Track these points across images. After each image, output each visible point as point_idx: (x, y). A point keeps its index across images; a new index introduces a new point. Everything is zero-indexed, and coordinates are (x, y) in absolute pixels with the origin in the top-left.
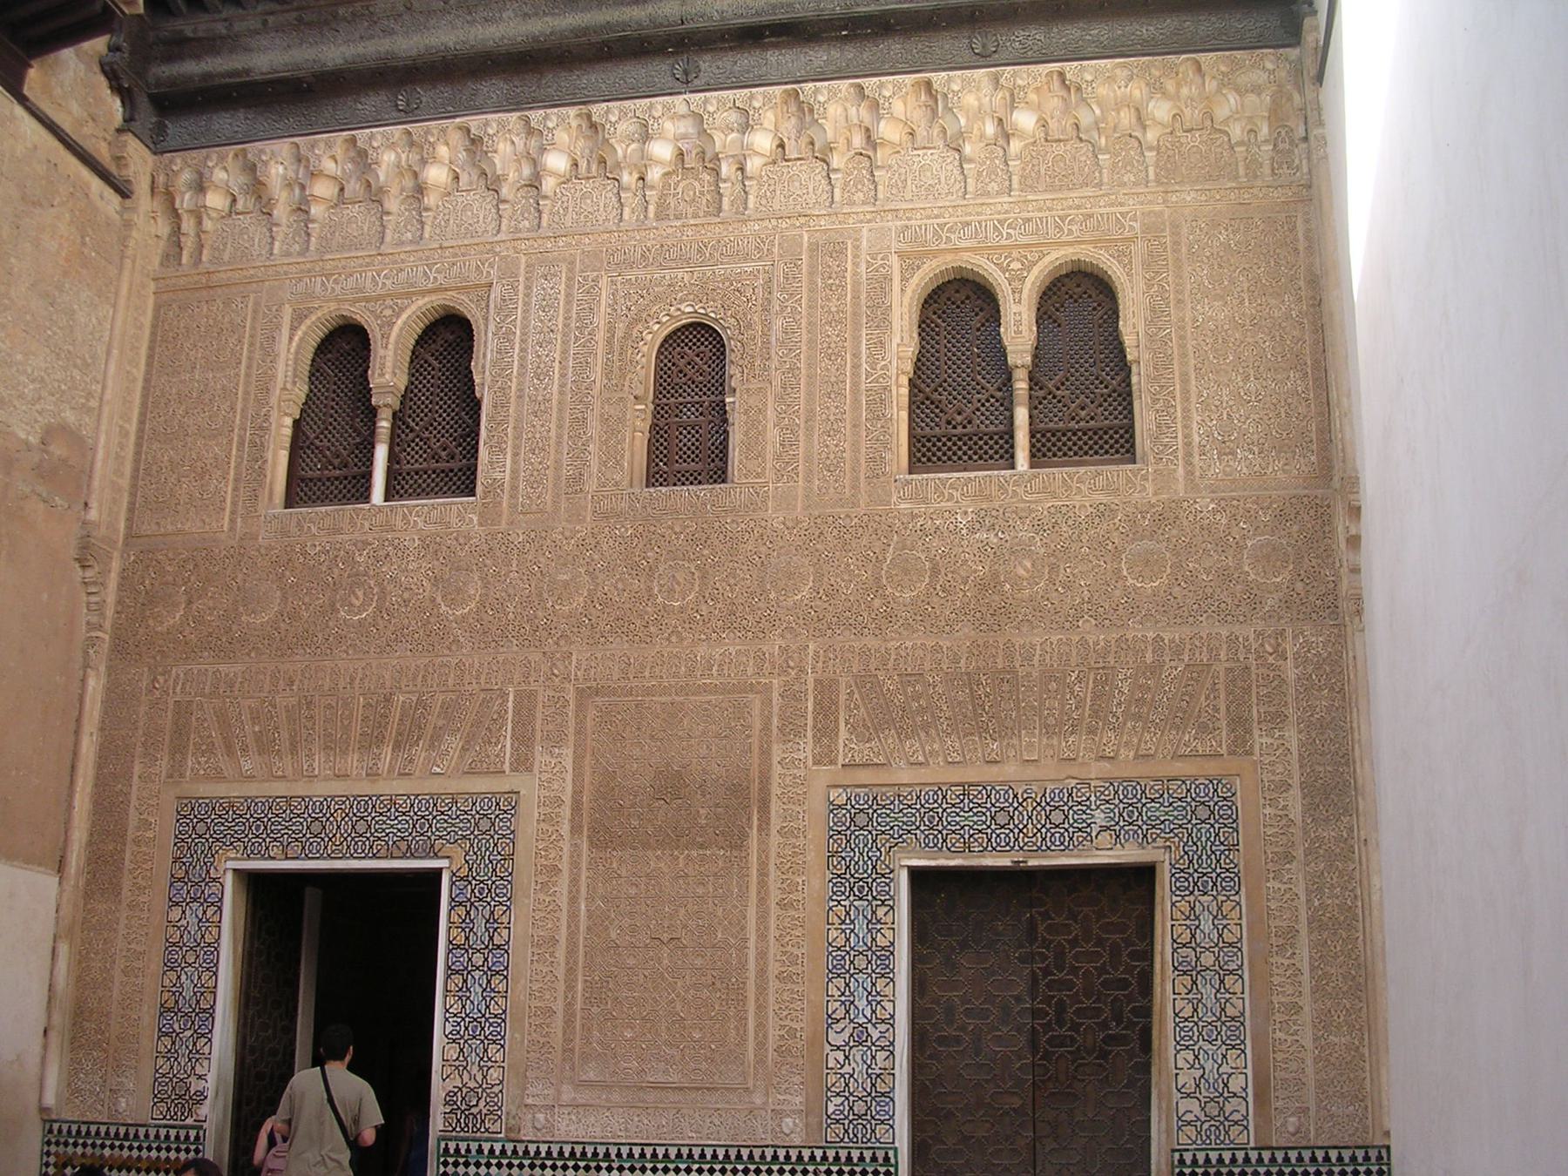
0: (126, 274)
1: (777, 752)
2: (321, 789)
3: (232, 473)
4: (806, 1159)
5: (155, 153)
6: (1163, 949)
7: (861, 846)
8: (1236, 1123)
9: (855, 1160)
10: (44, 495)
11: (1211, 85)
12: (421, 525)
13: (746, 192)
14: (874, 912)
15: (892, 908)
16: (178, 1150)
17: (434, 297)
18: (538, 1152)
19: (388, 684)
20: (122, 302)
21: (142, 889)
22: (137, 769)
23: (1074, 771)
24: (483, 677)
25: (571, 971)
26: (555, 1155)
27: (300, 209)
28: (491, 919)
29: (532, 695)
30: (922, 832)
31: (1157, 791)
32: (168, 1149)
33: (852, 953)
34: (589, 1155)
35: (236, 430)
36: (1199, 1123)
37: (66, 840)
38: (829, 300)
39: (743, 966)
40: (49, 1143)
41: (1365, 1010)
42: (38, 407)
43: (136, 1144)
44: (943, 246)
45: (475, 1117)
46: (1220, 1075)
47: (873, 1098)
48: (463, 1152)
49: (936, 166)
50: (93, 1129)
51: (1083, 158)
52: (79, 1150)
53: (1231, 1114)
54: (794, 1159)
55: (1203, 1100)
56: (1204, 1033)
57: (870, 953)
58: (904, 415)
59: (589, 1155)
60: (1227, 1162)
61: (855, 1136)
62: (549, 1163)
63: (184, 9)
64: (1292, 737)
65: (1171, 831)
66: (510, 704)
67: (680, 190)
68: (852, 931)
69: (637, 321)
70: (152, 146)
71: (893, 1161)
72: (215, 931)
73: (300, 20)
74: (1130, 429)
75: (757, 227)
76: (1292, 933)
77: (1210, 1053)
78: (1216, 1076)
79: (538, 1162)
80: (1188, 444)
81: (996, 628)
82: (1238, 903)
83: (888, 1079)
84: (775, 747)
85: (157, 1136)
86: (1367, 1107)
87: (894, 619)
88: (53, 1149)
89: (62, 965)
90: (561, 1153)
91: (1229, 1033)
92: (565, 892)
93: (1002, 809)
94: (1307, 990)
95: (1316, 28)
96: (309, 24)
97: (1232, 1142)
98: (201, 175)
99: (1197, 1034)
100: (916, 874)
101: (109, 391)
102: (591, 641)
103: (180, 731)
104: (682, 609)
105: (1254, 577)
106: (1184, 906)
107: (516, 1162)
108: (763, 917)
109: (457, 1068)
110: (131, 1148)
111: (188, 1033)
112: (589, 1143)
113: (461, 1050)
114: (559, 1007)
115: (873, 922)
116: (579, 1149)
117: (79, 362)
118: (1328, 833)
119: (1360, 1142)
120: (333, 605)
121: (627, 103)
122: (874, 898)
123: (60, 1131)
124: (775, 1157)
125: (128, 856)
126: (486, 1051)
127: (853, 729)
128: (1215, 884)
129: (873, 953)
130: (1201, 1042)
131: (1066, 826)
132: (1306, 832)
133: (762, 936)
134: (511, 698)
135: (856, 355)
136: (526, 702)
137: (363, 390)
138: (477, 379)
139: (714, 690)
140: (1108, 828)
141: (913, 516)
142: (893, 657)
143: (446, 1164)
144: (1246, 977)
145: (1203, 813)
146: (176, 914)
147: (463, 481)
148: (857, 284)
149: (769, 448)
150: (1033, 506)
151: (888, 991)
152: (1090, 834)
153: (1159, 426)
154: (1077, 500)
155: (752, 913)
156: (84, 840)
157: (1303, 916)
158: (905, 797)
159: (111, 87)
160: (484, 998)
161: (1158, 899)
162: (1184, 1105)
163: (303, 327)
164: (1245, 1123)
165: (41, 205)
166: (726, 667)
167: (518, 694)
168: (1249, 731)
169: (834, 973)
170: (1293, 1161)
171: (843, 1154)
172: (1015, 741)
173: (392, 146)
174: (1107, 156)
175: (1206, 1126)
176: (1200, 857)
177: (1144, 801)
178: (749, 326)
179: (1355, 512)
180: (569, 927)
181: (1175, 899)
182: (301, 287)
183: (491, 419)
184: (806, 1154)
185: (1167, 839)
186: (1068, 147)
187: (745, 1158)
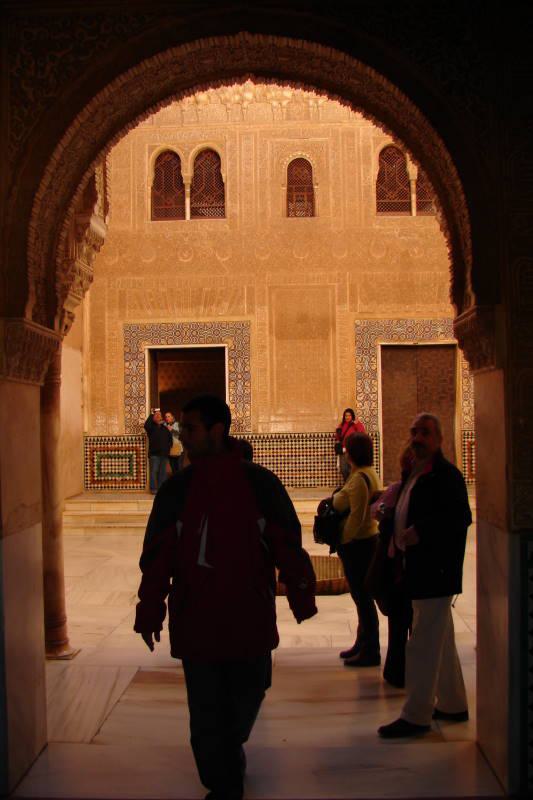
1: (337, 308)
2: (178, 321)
22: (107, 314)
25: (272, 379)
28: (244, 364)
39: (329, 377)
100: (383, 347)
108: (335, 361)
125: (107, 345)
127: (362, 301)
133: (335, 366)
135: (360, 174)
136: (251, 291)
138: (223, 175)
146: (127, 364)
155: (331, 360)
167: (248, 288)
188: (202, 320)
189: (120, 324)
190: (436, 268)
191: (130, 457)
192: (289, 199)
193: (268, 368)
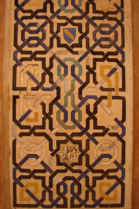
8: (105, 174)
36: (47, 175)
46: (83, 100)
53: (98, 160)
55: (55, 139)
56: (61, 35)
77: (69, 64)
78: (78, 102)
91: (99, 36)
99: (49, 35)
130: (55, 49)
164: (119, 174)
175: (58, 179)
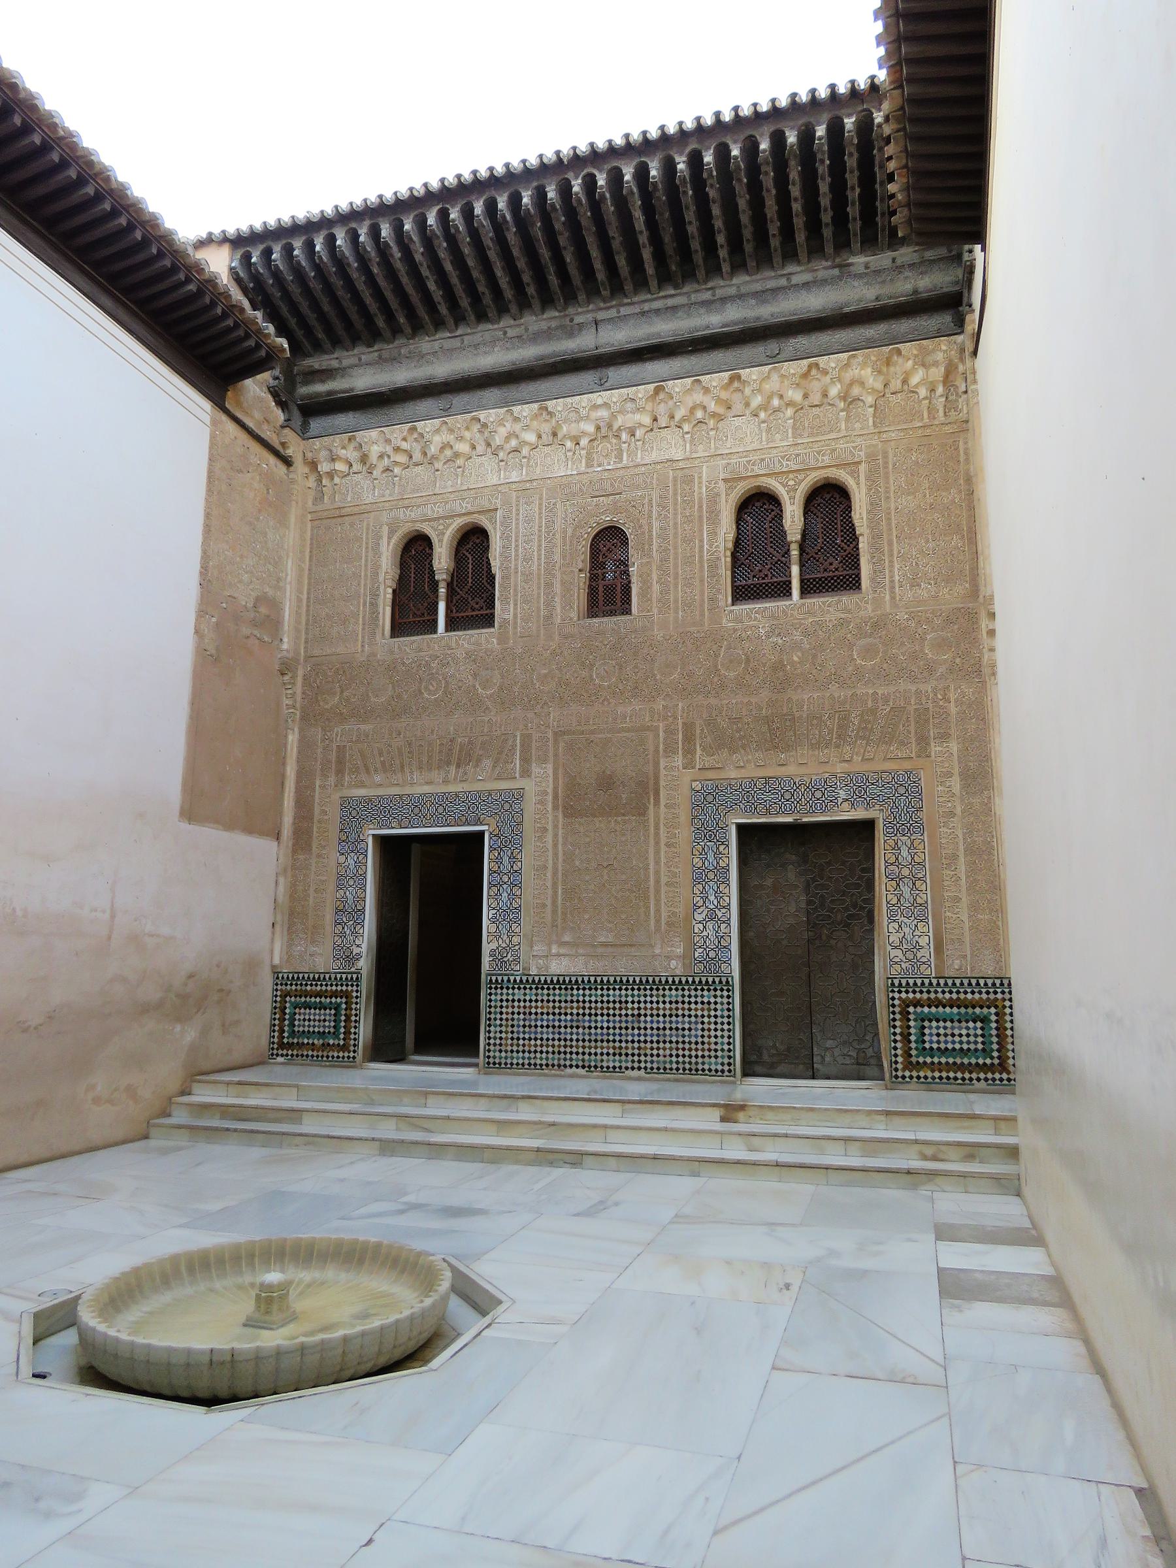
0: (293, 510)
1: (662, 763)
3: (361, 621)
4: (684, 982)
5: (304, 439)
6: (879, 864)
7: (710, 812)
8: (924, 963)
9: (710, 983)
10: (258, 635)
11: (910, 363)
12: (466, 646)
13: (637, 449)
14: (718, 848)
15: (728, 846)
16: (347, 985)
17: (465, 518)
18: (540, 981)
19: (452, 733)
20: (292, 526)
21: (324, 847)
22: (318, 783)
23: (828, 768)
24: (503, 727)
25: (555, 885)
26: (549, 982)
27: (388, 469)
28: (512, 858)
29: (529, 736)
30: (743, 804)
31: (875, 779)
32: (342, 985)
33: (706, 871)
34: (567, 982)
35: (362, 597)
37: (281, 823)
38: (685, 509)
39: (647, 879)
40: (277, 984)
41: (999, 900)
42: (251, 587)
43: (324, 983)
44: (751, 474)
45: (506, 962)
46: (914, 936)
47: (719, 949)
48: (500, 981)
49: (744, 426)
50: (301, 976)
51: (830, 415)
52: (294, 987)
54: (677, 982)
55: (904, 950)
57: (716, 871)
58: (729, 573)
59: (567, 982)
60: (919, 985)
61: (710, 969)
62: (546, 986)
63: (312, 352)
64: (954, 747)
65: (883, 801)
66: (518, 741)
67: (599, 449)
68: (706, 858)
69: (577, 527)
70: (301, 434)
71: (731, 983)
72: (364, 868)
73: (380, 357)
74: (858, 576)
75: (643, 469)
76: (955, 857)
79: (540, 986)
80: (892, 581)
81: (782, 690)
82: (923, 840)
83: (727, 939)
84: (662, 761)
85: (336, 978)
86: (1001, 955)
87: (725, 688)
88: (279, 987)
89: (281, 888)
90: (552, 981)
92: (551, 841)
93: (787, 790)
94: (964, 889)
95: (974, 321)
96: (386, 361)
97: (921, 974)
98: (331, 451)
100: (741, 828)
101: (289, 577)
102: (560, 706)
103: (340, 762)
104: (609, 687)
105: (930, 656)
106: (891, 842)
107: (528, 986)
108: (657, 852)
109: (496, 937)
110: (321, 985)
111: (351, 923)
112: (567, 975)
113: (498, 927)
114: (549, 902)
115: (718, 855)
116: (561, 979)
117: (272, 561)
118: (976, 801)
119: (997, 975)
120: (420, 691)
121: (569, 400)
122: (718, 841)
123: (283, 978)
124: (667, 982)
125: (315, 829)
126: (511, 927)
127: (704, 749)
128: (909, 830)
129: (718, 870)
131: (823, 799)
132: (962, 800)
133: (657, 863)
134: (518, 738)
135: (701, 541)
136: (526, 740)
137: (432, 573)
139: (628, 730)
140: (847, 800)
141: (735, 630)
142: (725, 709)
143: (491, 988)
144: (928, 881)
145: (902, 790)
147: (488, 620)
148: (700, 499)
149: (654, 595)
150: (803, 621)
151: (727, 891)
152: (837, 804)
153: (875, 572)
154: (828, 617)
155: (651, 850)
156: (291, 821)
157: (961, 848)
158: (733, 786)
159: (275, 402)
160: (509, 899)
161: (876, 839)
162: (894, 953)
163: (395, 537)
165: (242, 472)
166: (634, 717)
167: (522, 735)
168: (928, 744)
169: (696, 881)
170: (958, 985)
171: (704, 980)
172: (793, 753)
173: (437, 431)
174: (845, 413)
176: (900, 815)
177: (867, 784)
178: (641, 527)
179: (992, 616)
180: (553, 860)
181: (886, 838)
182: (392, 514)
183: (501, 585)
184: (684, 979)
185: (881, 806)
186: (822, 409)
187: (651, 982)
188: (452, 788)
189: (336, 797)
190: (834, 687)
191: (337, 1007)
192: (592, 592)
193: (550, 865)
